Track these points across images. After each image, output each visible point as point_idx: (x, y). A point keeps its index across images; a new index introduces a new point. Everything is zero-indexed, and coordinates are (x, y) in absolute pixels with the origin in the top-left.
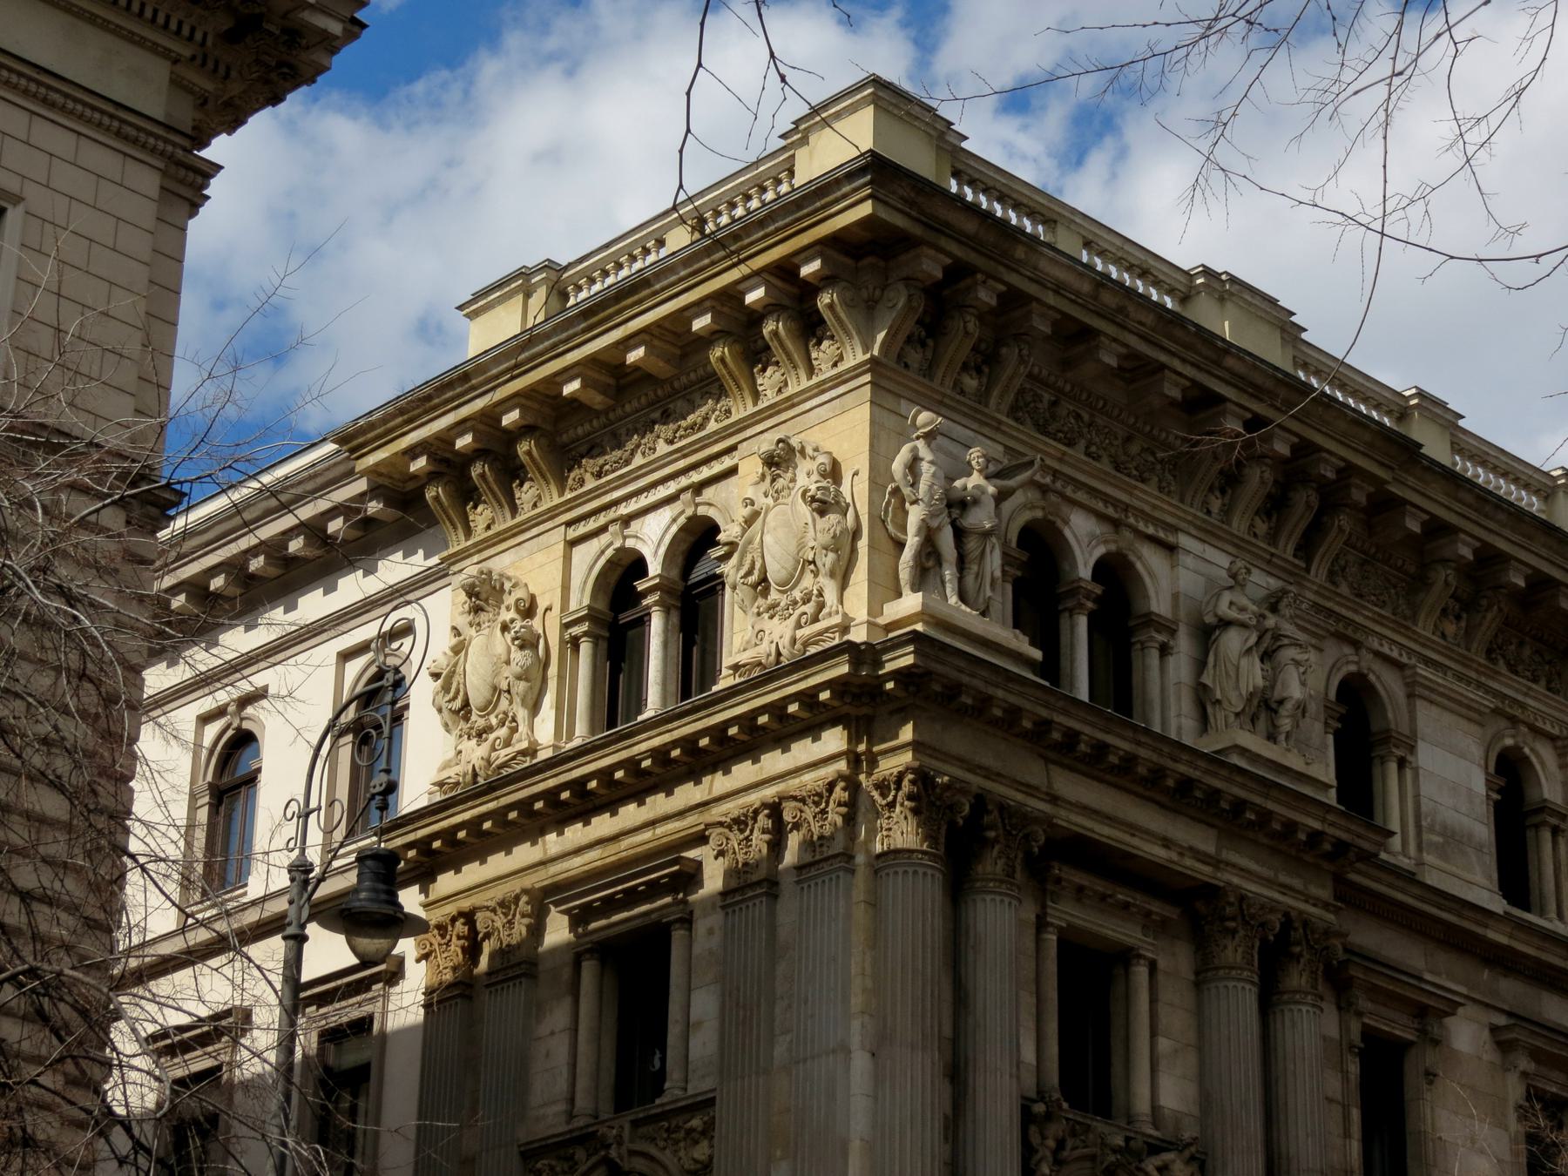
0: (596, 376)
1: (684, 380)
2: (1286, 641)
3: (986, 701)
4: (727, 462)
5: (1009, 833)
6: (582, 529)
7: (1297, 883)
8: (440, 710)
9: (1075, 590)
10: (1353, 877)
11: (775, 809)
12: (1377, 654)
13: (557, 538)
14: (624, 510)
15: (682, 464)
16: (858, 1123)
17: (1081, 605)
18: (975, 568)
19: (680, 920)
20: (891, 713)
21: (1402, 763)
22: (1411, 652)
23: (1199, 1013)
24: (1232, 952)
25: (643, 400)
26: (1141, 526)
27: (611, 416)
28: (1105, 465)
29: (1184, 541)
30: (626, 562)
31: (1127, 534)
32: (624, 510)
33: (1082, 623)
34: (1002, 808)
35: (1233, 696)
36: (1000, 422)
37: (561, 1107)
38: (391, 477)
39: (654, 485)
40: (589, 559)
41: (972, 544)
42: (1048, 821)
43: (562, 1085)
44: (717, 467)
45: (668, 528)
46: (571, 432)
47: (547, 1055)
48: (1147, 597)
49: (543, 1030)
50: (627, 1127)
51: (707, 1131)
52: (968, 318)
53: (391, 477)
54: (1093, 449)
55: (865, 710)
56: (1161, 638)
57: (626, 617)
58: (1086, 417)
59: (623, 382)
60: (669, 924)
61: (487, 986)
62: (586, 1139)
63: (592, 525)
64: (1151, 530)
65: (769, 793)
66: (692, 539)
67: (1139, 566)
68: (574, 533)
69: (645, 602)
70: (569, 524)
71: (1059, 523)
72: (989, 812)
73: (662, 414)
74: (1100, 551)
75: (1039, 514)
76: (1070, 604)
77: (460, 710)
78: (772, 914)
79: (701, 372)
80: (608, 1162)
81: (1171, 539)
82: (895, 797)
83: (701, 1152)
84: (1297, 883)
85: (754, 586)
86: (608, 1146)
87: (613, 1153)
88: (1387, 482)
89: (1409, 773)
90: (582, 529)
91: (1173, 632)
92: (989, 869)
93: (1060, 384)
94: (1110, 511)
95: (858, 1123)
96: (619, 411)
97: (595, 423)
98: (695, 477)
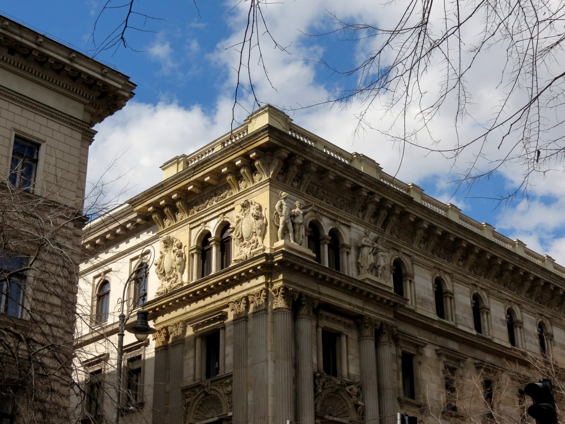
0: (197, 185)
1: (220, 185)
2: (380, 250)
3: (301, 268)
4: (232, 207)
5: (308, 303)
6: (194, 225)
7: (384, 314)
8: (157, 274)
9: (324, 238)
10: (398, 312)
11: (246, 298)
12: (404, 253)
13: (187, 227)
14: (205, 220)
15: (220, 207)
16: (271, 381)
17: (326, 242)
18: (298, 233)
19: (222, 328)
20: (277, 272)
21: (411, 281)
22: (412, 252)
24: (368, 332)
25: (209, 191)
26: (341, 221)
27: (201, 195)
28: (332, 205)
29: (352, 224)
30: (206, 233)
31: (337, 223)
32: (205, 220)
33: (326, 247)
34: (306, 296)
35: (366, 265)
36: (303, 194)
37: (192, 378)
39: (213, 213)
40: (196, 233)
41: (297, 227)
42: (318, 299)
43: (192, 372)
44: (229, 208)
46: (191, 200)
47: (188, 364)
48: (343, 239)
49: (187, 357)
51: (231, 383)
52: (294, 167)
54: (328, 201)
55: (270, 271)
56: (347, 250)
57: (206, 248)
58: (326, 193)
59: (204, 186)
60: (219, 329)
61: (172, 346)
62: (198, 386)
63: (196, 224)
64: (344, 222)
65: (245, 293)
66: (223, 227)
67: (341, 231)
68: (192, 226)
69: (211, 244)
70: (190, 224)
71: (320, 221)
72: (303, 297)
74: (331, 228)
75: (314, 218)
76: (323, 242)
78: (246, 325)
79: (224, 183)
80: (204, 392)
81: (349, 224)
83: (229, 389)
84: (384, 314)
85: (240, 239)
86: (204, 388)
87: (206, 390)
88: (405, 208)
89: (412, 284)
90: (194, 225)
91: (350, 249)
92: (303, 312)
93: (319, 184)
94: (333, 217)
95: (271, 381)
96: (203, 194)
97: (197, 197)
98: (224, 211)
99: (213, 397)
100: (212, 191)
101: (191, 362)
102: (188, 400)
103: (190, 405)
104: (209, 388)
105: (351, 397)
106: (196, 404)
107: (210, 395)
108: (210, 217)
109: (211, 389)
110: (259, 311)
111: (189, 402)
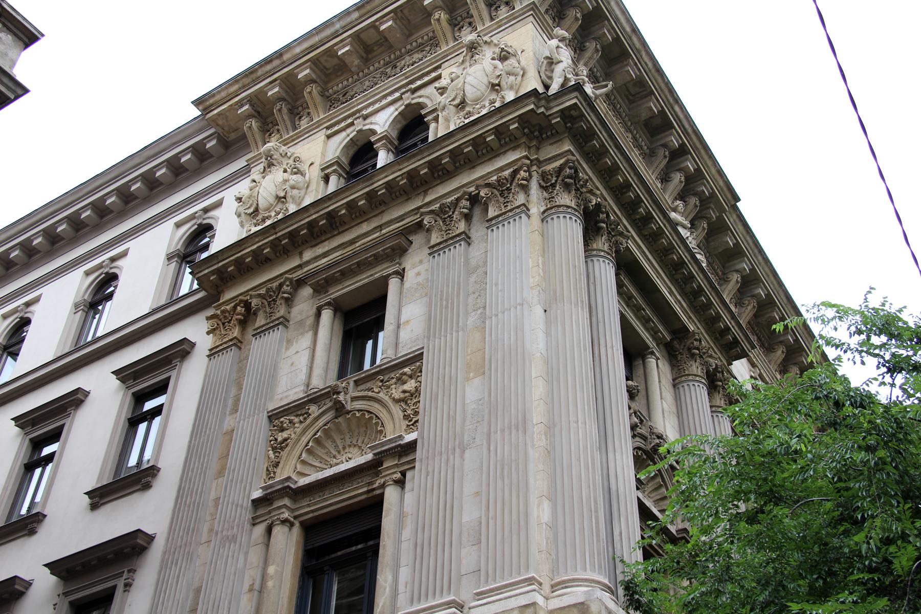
1: (409, 47)
3: (604, 152)
8: (239, 216)
23: (677, 399)
24: (695, 368)
25: (382, 62)
30: (360, 143)
32: (365, 112)
38: (223, 129)
39: (385, 97)
40: (336, 145)
43: (302, 376)
45: (393, 113)
46: (335, 88)
47: (292, 364)
50: (352, 384)
51: (416, 375)
53: (223, 129)
59: (370, 56)
61: (253, 335)
66: (404, 123)
68: (329, 132)
70: (328, 128)
73: (392, 68)
77: (252, 213)
78: (466, 253)
82: (556, 181)
83: (410, 385)
85: (457, 106)
86: (339, 393)
87: (341, 397)
97: (350, 80)
98: (413, 86)
99: (358, 415)
100: (386, 64)
101: (303, 359)
102: (281, 437)
103: (287, 445)
106: (304, 439)
107: (348, 412)
108: (377, 106)
109: (354, 399)
110: (505, 213)
111: (285, 440)
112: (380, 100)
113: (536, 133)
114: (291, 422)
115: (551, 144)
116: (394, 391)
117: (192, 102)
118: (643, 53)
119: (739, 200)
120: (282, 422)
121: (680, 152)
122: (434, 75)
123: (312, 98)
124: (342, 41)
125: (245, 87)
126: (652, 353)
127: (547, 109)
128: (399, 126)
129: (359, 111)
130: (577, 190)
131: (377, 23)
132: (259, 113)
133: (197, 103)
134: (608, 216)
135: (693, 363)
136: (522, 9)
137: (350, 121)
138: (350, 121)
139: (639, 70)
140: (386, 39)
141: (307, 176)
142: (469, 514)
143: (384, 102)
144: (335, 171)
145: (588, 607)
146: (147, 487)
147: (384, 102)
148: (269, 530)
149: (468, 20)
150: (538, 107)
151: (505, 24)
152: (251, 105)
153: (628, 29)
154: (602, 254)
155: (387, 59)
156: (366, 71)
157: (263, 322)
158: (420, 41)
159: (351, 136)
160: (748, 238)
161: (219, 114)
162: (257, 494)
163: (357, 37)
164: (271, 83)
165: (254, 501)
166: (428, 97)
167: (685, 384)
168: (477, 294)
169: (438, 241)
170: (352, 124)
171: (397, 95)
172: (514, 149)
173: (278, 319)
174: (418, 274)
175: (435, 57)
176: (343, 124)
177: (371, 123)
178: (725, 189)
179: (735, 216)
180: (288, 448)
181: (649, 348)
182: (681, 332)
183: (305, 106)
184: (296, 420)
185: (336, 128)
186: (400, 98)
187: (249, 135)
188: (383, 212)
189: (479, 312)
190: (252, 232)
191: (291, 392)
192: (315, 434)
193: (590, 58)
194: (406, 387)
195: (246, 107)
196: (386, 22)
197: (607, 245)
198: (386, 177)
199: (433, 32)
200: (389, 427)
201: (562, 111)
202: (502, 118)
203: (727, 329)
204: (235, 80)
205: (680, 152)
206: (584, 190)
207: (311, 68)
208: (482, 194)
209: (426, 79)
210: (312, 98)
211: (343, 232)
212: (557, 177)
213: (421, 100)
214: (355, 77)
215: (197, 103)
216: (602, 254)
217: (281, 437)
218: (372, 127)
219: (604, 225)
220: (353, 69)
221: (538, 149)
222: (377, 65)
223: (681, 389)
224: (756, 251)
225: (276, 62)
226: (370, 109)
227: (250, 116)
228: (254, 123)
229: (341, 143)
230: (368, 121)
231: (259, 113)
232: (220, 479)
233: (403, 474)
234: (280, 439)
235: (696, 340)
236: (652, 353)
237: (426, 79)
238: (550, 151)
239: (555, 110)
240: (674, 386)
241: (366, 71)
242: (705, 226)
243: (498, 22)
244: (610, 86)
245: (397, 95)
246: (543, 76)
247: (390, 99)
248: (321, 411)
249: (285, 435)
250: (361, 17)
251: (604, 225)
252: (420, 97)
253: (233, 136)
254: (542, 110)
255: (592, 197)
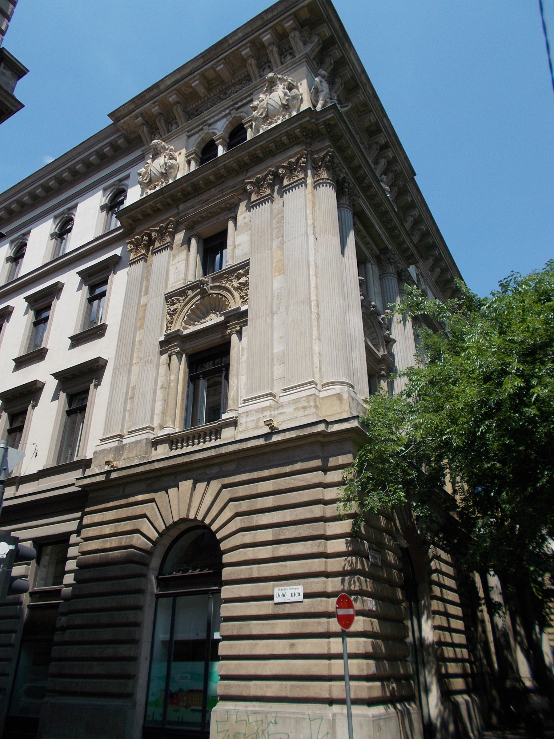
1: (233, 81)
24: (391, 269)
25: (218, 91)
30: (208, 140)
32: (209, 122)
38: (127, 131)
39: (221, 112)
43: (182, 275)
46: (191, 107)
51: (247, 273)
53: (127, 131)
55: (309, 141)
59: (211, 87)
62: (193, 287)
66: (232, 128)
68: (189, 134)
70: (188, 132)
86: (203, 285)
97: (200, 102)
98: (237, 106)
99: (214, 296)
101: (182, 265)
102: (172, 308)
103: (176, 312)
104: (209, 286)
105: (381, 328)
108: (216, 118)
109: (212, 288)
110: (293, 183)
111: (175, 310)
112: (218, 115)
113: (310, 135)
114: (178, 299)
115: (318, 142)
116: (234, 283)
117: (108, 115)
118: (368, 86)
119: (415, 175)
120: (173, 300)
121: (385, 147)
122: (249, 99)
123: (178, 112)
124: (194, 77)
125: (137, 107)
126: (370, 261)
127: (317, 120)
128: (229, 130)
129: (206, 121)
130: (333, 169)
131: (215, 66)
132: (147, 122)
133: (111, 115)
134: (349, 184)
135: (390, 266)
136: (300, 57)
137: (201, 127)
138: (201, 127)
139: (365, 96)
140: (220, 76)
141: (178, 160)
142: (278, 348)
143: (220, 116)
144: (193, 158)
145: (342, 396)
146: (102, 335)
147: (220, 116)
148: (170, 356)
149: (268, 64)
150: (311, 119)
151: (290, 66)
152: (143, 117)
153: (359, 71)
154: (346, 206)
155: (221, 89)
156: (209, 96)
157: (159, 245)
158: (240, 77)
159: (202, 136)
160: (419, 197)
161: (124, 123)
162: (162, 338)
163: (203, 75)
164: (154, 103)
165: (160, 342)
166: (245, 113)
167: (386, 278)
168: (278, 229)
169: (256, 199)
170: (202, 129)
171: (227, 111)
172: (297, 144)
173: (167, 243)
174: (245, 218)
175: (249, 88)
176: (197, 129)
177: (213, 129)
178: (408, 168)
179: (412, 184)
180: (177, 315)
181: (368, 259)
182: (384, 250)
183: (174, 118)
184: (181, 299)
185: (192, 132)
186: (230, 113)
187: (142, 135)
188: (223, 182)
189: (279, 239)
190: (149, 194)
191: (177, 284)
192: (192, 306)
193: (338, 89)
194: (241, 281)
195: (140, 118)
196: (220, 65)
197: (348, 201)
198: (224, 161)
199: (248, 72)
200: (232, 302)
201: (325, 121)
202: (290, 125)
203: (408, 248)
204: (132, 101)
205: (385, 147)
206: (337, 169)
207: (176, 94)
208: (280, 171)
209: (244, 101)
210: (178, 112)
211: (201, 193)
212: (322, 162)
213: (242, 114)
214: (203, 100)
215: (111, 115)
216: (346, 206)
217: (172, 308)
218: (214, 131)
219: (347, 190)
220: (201, 95)
221: (311, 144)
222: (215, 92)
223: (384, 281)
224: (423, 205)
225: (155, 91)
226: (212, 120)
227: (142, 124)
228: (145, 128)
229: (196, 141)
230: (211, 127)
231: (147, 122)
232: (141, 331)
233: (241, 328)
234: (172, 309)
235: (392, 254)
236: (370, 261)
237: (244, 101)
238: (317, 146)
239: (321, 120)
240: (380, 279)
241: (209, 96)
242: (396, 190)
243: (286, 66)
244: (349, 106)
245: (227, 111)
246: (313, 100)
247: (223, 114)
248: (194, 293)
249: (175, 306)
250: (204, 62)
251: (347, 190)
252: (241, 112)
253: (133, 136)
254: (314, 120)
255: (341, 173)
